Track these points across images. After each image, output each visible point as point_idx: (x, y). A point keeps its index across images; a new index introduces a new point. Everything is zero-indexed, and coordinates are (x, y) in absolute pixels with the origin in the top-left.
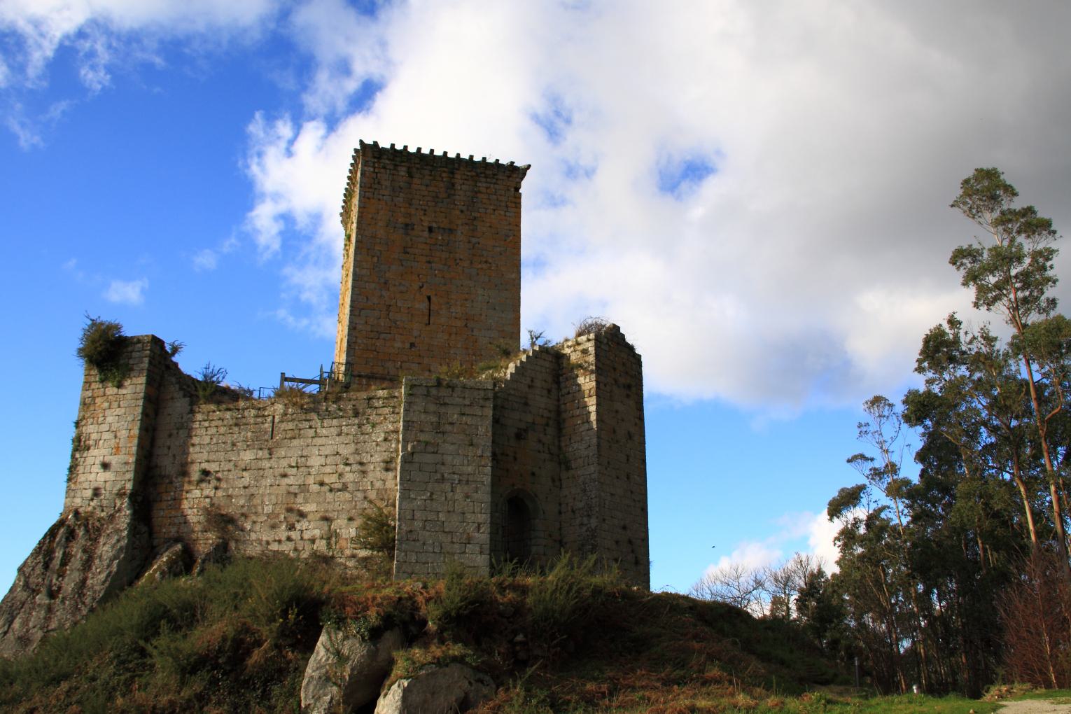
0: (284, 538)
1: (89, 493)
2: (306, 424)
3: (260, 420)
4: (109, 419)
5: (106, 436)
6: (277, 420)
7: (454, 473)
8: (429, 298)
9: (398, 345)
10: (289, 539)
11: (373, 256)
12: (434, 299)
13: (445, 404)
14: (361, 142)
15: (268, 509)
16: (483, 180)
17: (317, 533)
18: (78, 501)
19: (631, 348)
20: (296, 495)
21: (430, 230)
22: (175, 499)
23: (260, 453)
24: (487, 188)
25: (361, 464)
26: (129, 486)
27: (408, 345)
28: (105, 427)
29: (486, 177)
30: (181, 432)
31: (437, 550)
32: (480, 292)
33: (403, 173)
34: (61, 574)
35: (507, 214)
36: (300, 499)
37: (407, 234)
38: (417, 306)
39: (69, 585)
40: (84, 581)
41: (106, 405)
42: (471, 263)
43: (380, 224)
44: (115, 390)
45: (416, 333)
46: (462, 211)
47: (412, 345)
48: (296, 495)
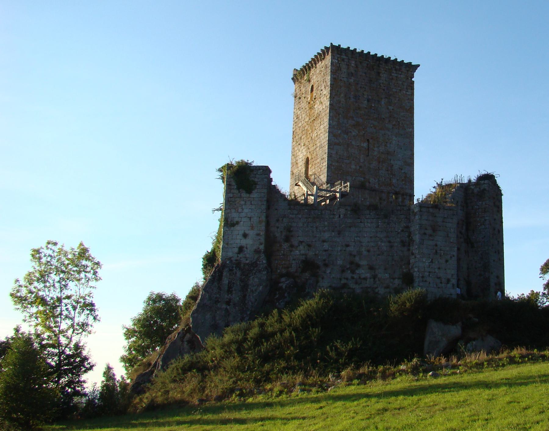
0: (350, 277)
1: (236, 250)
2: (359, 221)
3: (332, 216)
4: (246, 211)
5: (244, 220)
6: (341, 216)
7: (441, 250)
8: (368, 140)
9: (353, 167)
10: (353, 278)
11: (339, 114)
12: (371, 141)
13: (435, 216)
14: (331, 44)
15: (340, 262)
16: (395, 72)
17: (368, 275)
18: (230, 254)
19: (498, 187)
20: (355, 256)
21: (368, 100)
22: (284, 255)
23: (333, 234)
24: (397, 77)
25: (390, 242)
26: (262, 247)
27: (358, 168)
28: (243, 215)
29: (396, 70)
30: (284, 219)
31: (435, 286)
32: (394, 138)
33: (353, 65)
34: (229, 291)
35: (408, 93)
36: (357, 259)
37: (356, 102)
38: (362, 145)
39: (236, 297)
40: (245, 296)
41: (243, 203)
42: (389, 121)
43: (342, 95)
44: (248, 195)
45: (362, 161)
46: (384, 90)
47: (361, 167)
48: (355, 256)
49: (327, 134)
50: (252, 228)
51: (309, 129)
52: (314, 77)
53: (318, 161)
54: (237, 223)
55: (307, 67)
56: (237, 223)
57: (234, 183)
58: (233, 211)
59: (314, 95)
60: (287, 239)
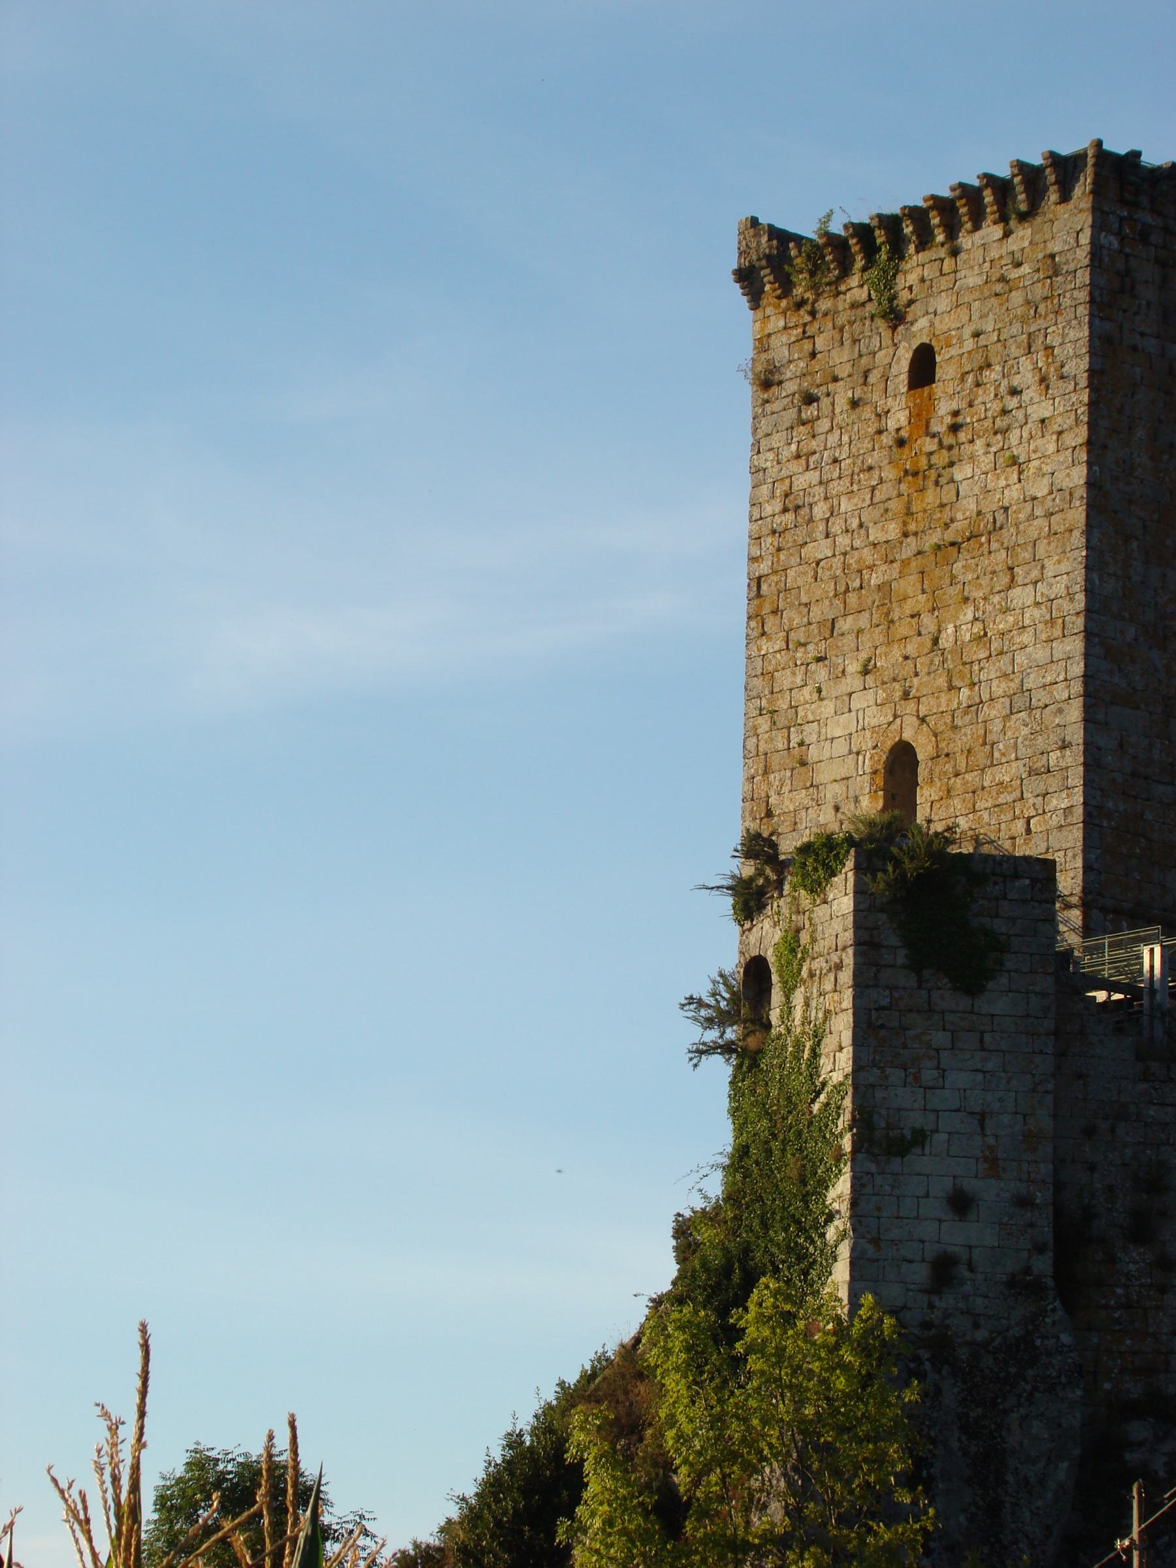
1: (920, 1273)
26: (1043, 1265)
41: (940, 1038)
43: (1140, 433)
44: (964, 1002)
49: (1075, 646)
50: (993, 1166)
51: (909, 584)
52: (943, 303)
53: (1004, 774)
54: (920, 1138)
55: (880, 237)
56: (920, 1138)
57: (892, 939)
58: (896, 1075)
59: (944, 408)
60: (1141, 1230)
